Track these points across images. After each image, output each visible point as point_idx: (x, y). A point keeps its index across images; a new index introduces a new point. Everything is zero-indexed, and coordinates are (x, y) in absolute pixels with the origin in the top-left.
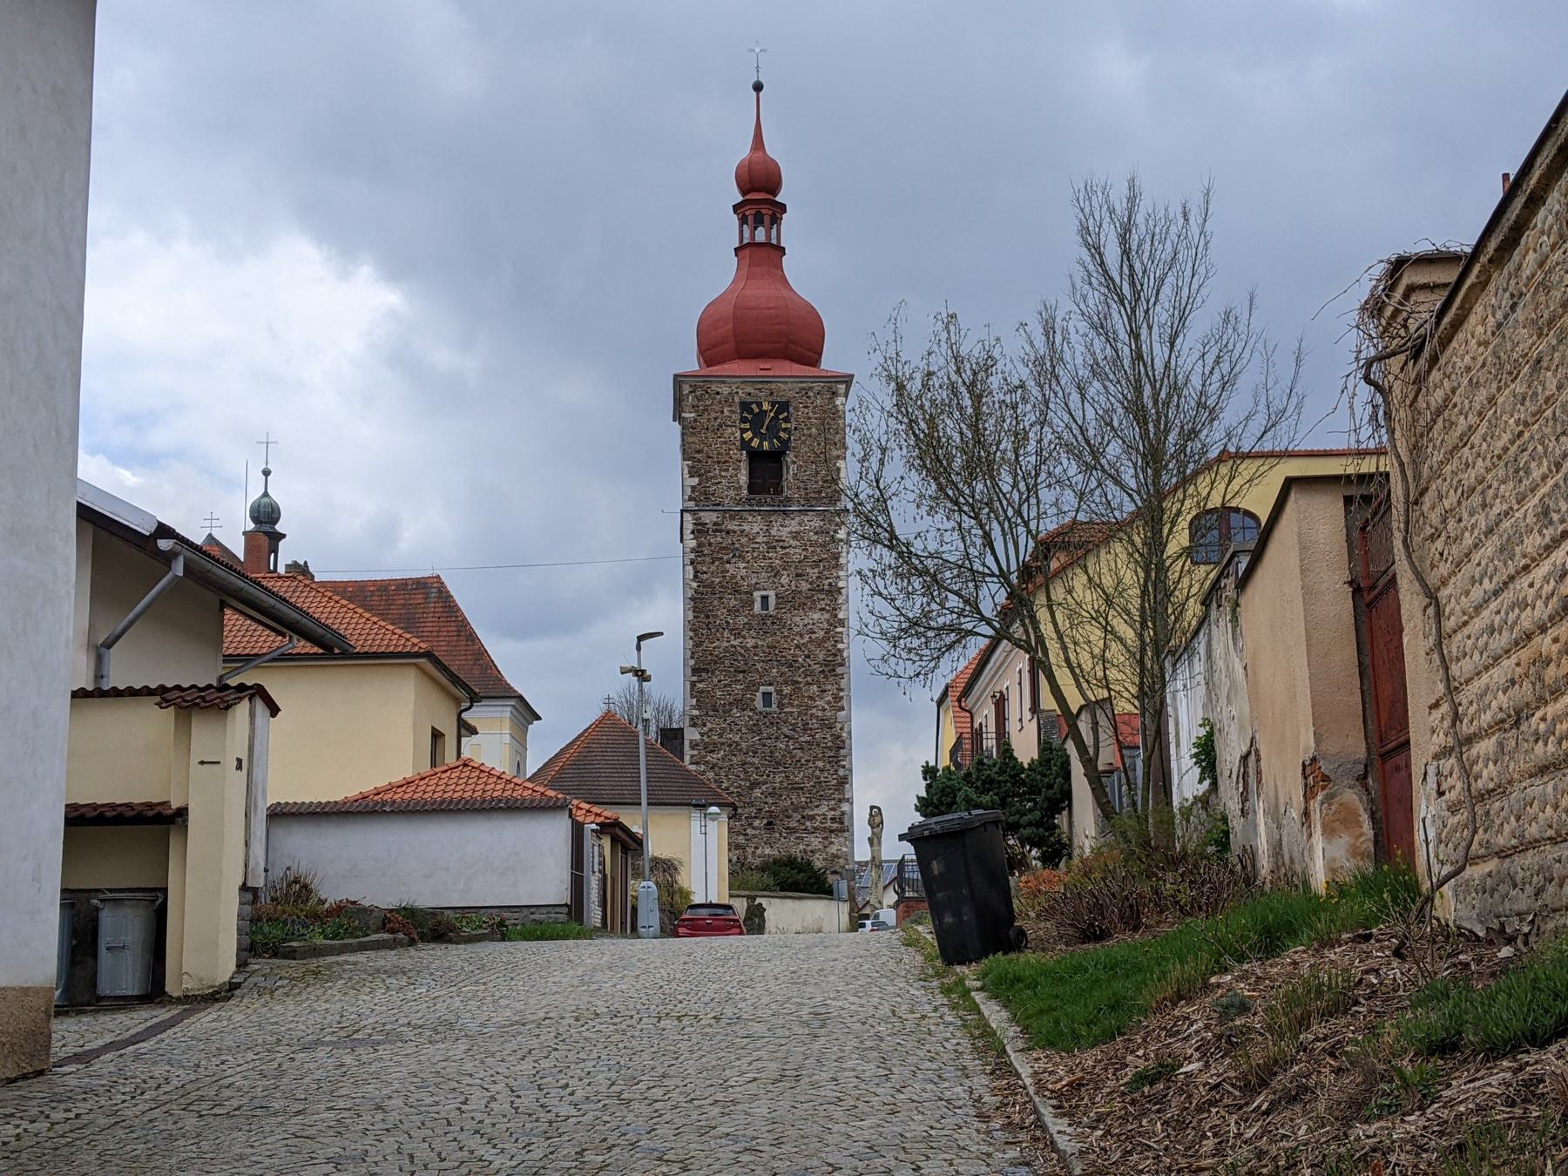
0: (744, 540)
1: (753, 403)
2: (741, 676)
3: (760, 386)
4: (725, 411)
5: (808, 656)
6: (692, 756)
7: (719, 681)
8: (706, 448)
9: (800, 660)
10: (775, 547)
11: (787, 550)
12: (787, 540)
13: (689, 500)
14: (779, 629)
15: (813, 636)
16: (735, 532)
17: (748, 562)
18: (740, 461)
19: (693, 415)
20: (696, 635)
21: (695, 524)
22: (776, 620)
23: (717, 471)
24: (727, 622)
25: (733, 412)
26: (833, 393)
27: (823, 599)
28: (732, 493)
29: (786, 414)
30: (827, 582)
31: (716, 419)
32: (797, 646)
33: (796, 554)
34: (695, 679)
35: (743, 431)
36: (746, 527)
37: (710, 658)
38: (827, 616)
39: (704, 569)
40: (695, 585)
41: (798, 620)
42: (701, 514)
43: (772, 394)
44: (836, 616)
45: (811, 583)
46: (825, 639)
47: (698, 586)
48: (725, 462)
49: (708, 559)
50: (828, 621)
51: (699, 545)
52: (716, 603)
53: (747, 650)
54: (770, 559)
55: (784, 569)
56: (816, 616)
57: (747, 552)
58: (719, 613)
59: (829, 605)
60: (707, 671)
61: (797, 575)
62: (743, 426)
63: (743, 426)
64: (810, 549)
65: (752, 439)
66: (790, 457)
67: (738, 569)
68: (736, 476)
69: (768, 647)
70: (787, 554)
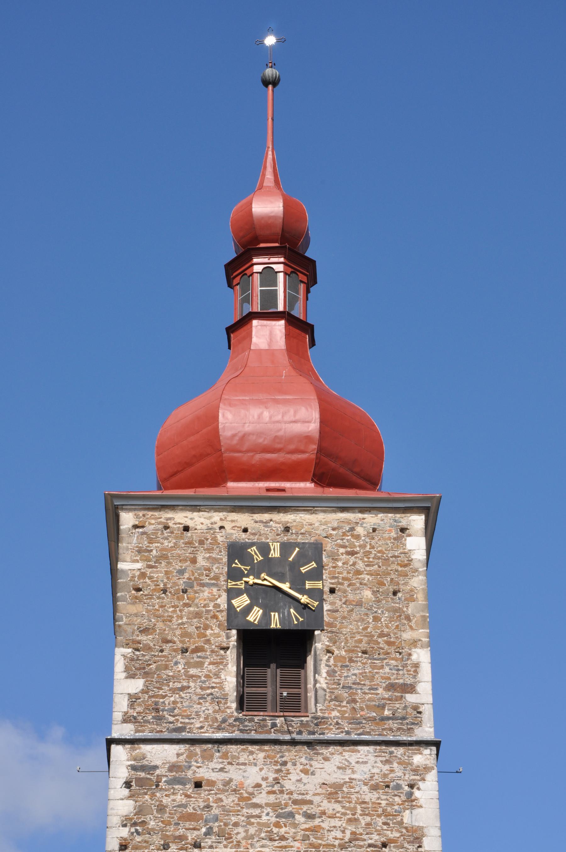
0: (229, 800)
1: (252, 544)
3: (266, 517)
4: (200, 559)
8: (160, 625)
10: (291, 815)
11: (317, 822)
12: (317, 799)
16: (212, 783)
18: (226, 649)
19: (138, 565)
23: (180, 667)
25: (215, 561)
26: (403, 530)
28: (208, 708)
29: (314, 565)
31: (181, 572)
35: (232, 593)
36: (234, 774)
42: (146, 748)
43: (287, 529)
48: (197, 650)
51: (140, 811)
54: (283, 838)
57: (236, 824)
63: (231, 584)
64: (364, 820)
65: (248, 610)
68: (217, 675)
70: (315, 830)
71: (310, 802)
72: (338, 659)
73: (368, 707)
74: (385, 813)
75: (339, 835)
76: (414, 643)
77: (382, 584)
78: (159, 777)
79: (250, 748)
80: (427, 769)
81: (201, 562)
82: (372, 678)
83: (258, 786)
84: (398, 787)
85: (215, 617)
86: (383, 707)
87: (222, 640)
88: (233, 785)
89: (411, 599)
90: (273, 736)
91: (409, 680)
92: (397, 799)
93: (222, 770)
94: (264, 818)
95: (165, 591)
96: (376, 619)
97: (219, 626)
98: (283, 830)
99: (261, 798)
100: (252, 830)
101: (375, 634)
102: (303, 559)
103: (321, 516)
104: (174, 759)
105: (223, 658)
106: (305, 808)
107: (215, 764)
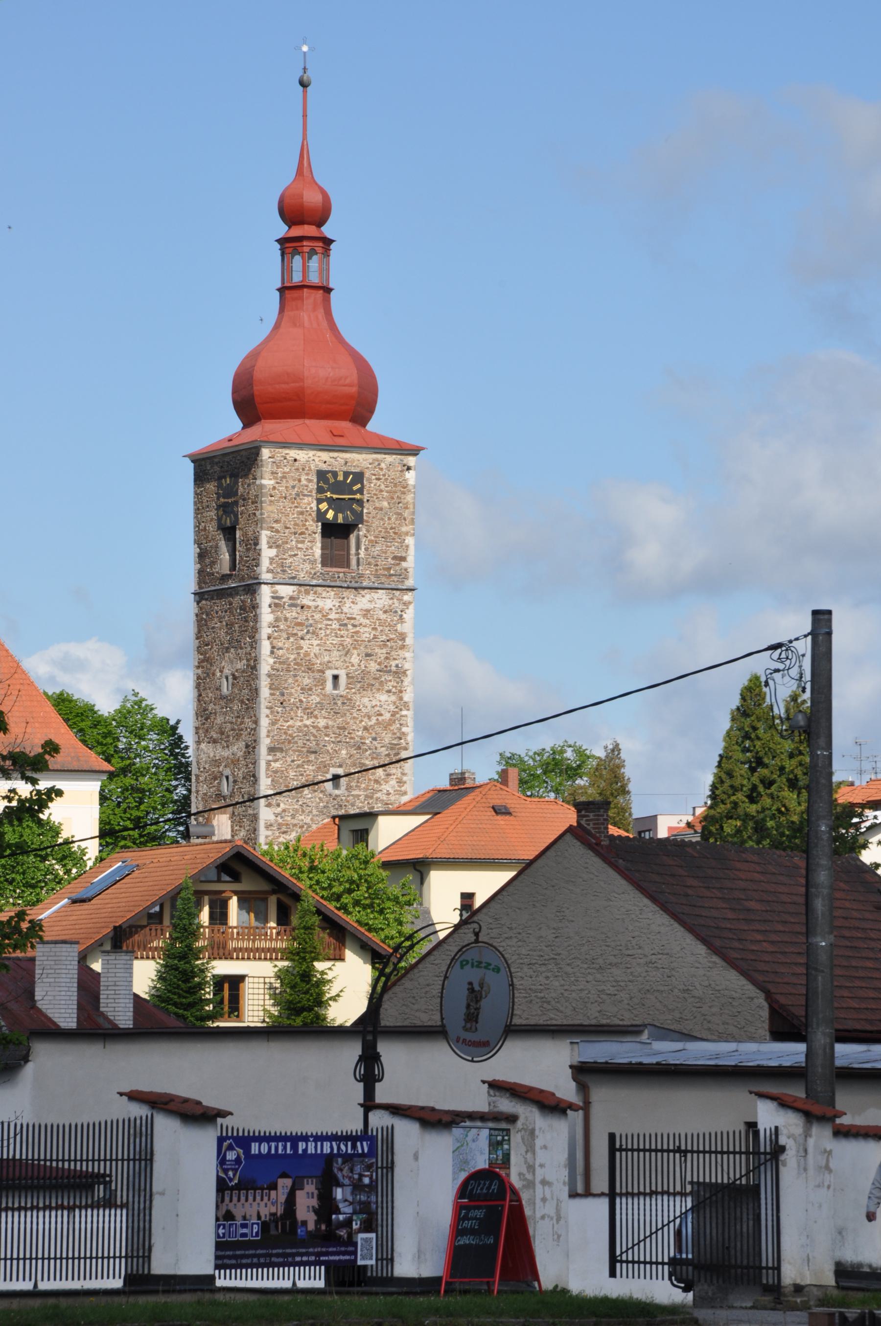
0: (317, 616)
2: (312, 757)
3: (335, 454)
4: (303, 479)
5: (375, 739)
6: (267, 837)
7: (293, 761)
9: (367, 742)
10: (346, 625)
11: (358, 629)
12: (358, 617)
13: (268, 572)
14: (348, 710)
15: (380, 718)
16: (309, 607)
17: (321, 639)
18: (315, 533)
20: (272, 712)
21: (273, 597)
22: (347, 701)
23: (294, 543)
24: (301, 701)
25: (309, 481)
27: (390, 681)
28: (307, 566)
29: (359, 486)
30: (393, 663)
31: (293, 487)
32: (366, 729)
33: (366, 634)
34: (270, 758)
35: (319, 501)
36: (320, 603)
37: (284, 737)
38: (393, 698)
39: (280, 645)
40: (271, 661)
41: (365, 701)
42: (278, 587)
43: (346, 463)
44: (401, 699)
45: (379, 664)
46: (391, 722)
47: (275, 663)
48: (302, 533)
49: (285, 635)
50: (394, 703)
51: (277, 620)
52: (290, 681)
53: (319, 730)
54: (342, 637)
55: (355, 648)
56: (383, 697)
57: (321, 629)
58: (293, 691)
59: (396, 687)
60: (281, 750)
61: (368, 655)
62: (319, 496)
63: (319, 496)
64: (380, 628)
66: (363, 530)
67: (312, 646)
68: (311, 548)
69: (339, 728)
70: (357, 632)
71: (355, 619)
72: (370, 541)
73: (384, 569)
74: (390, 625)
75: (368, 636)
76: (407, 534)
77: (393, 498)
78: (284, 603)
79: (328, 589)
80: (410, 603)
81: (304, 482)
82: (386, 553)
83: (331, 609)
84: (396, 612)
85: (310, 515)
86: (390, 569)
87: (314, 528)
88: (319, 608)
89: (406, 508)
90: (338, 583)
91: (404, 555)
92: (395, 618)
93: (314, 600)
94: (334, 626)
95: (285, 498)
96: (389, 519)
97: (313, 520)
98: (342, 632)
99: (332, 616)
100: (328, 632)
101: (388, 527)
102: (354, 482)
103: (364, 456)
104: (291, 594)
105: (315, 538)
106: (352, 621)
107: (311, 597)
